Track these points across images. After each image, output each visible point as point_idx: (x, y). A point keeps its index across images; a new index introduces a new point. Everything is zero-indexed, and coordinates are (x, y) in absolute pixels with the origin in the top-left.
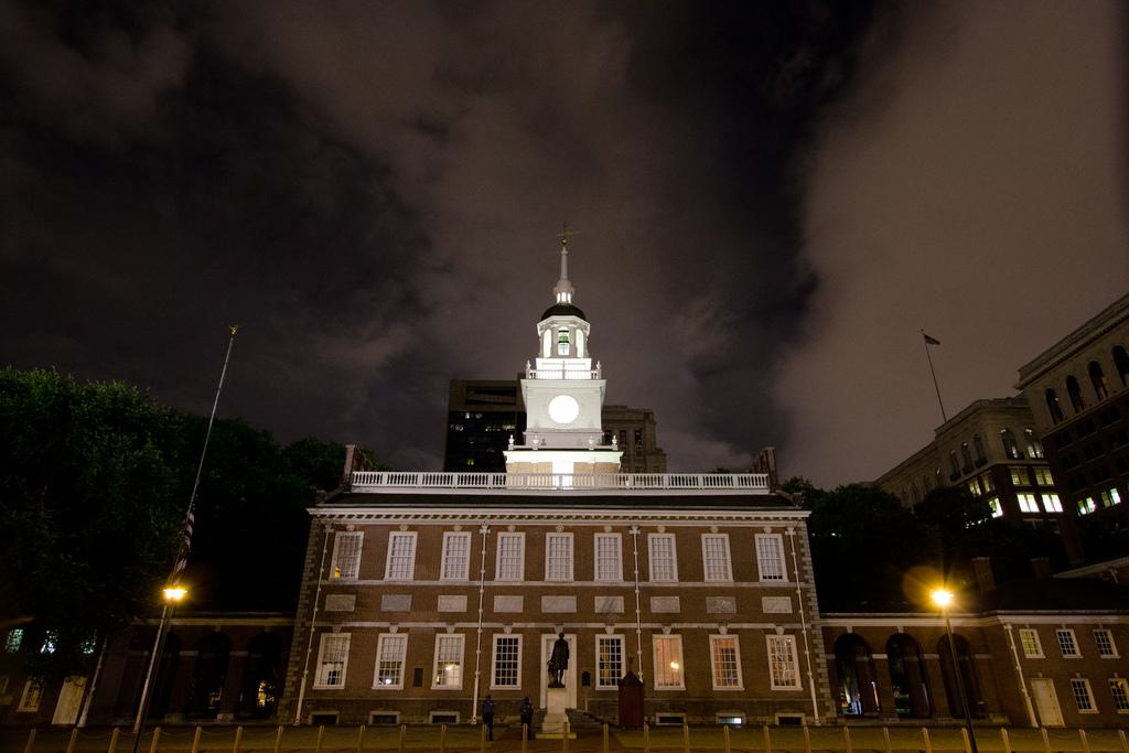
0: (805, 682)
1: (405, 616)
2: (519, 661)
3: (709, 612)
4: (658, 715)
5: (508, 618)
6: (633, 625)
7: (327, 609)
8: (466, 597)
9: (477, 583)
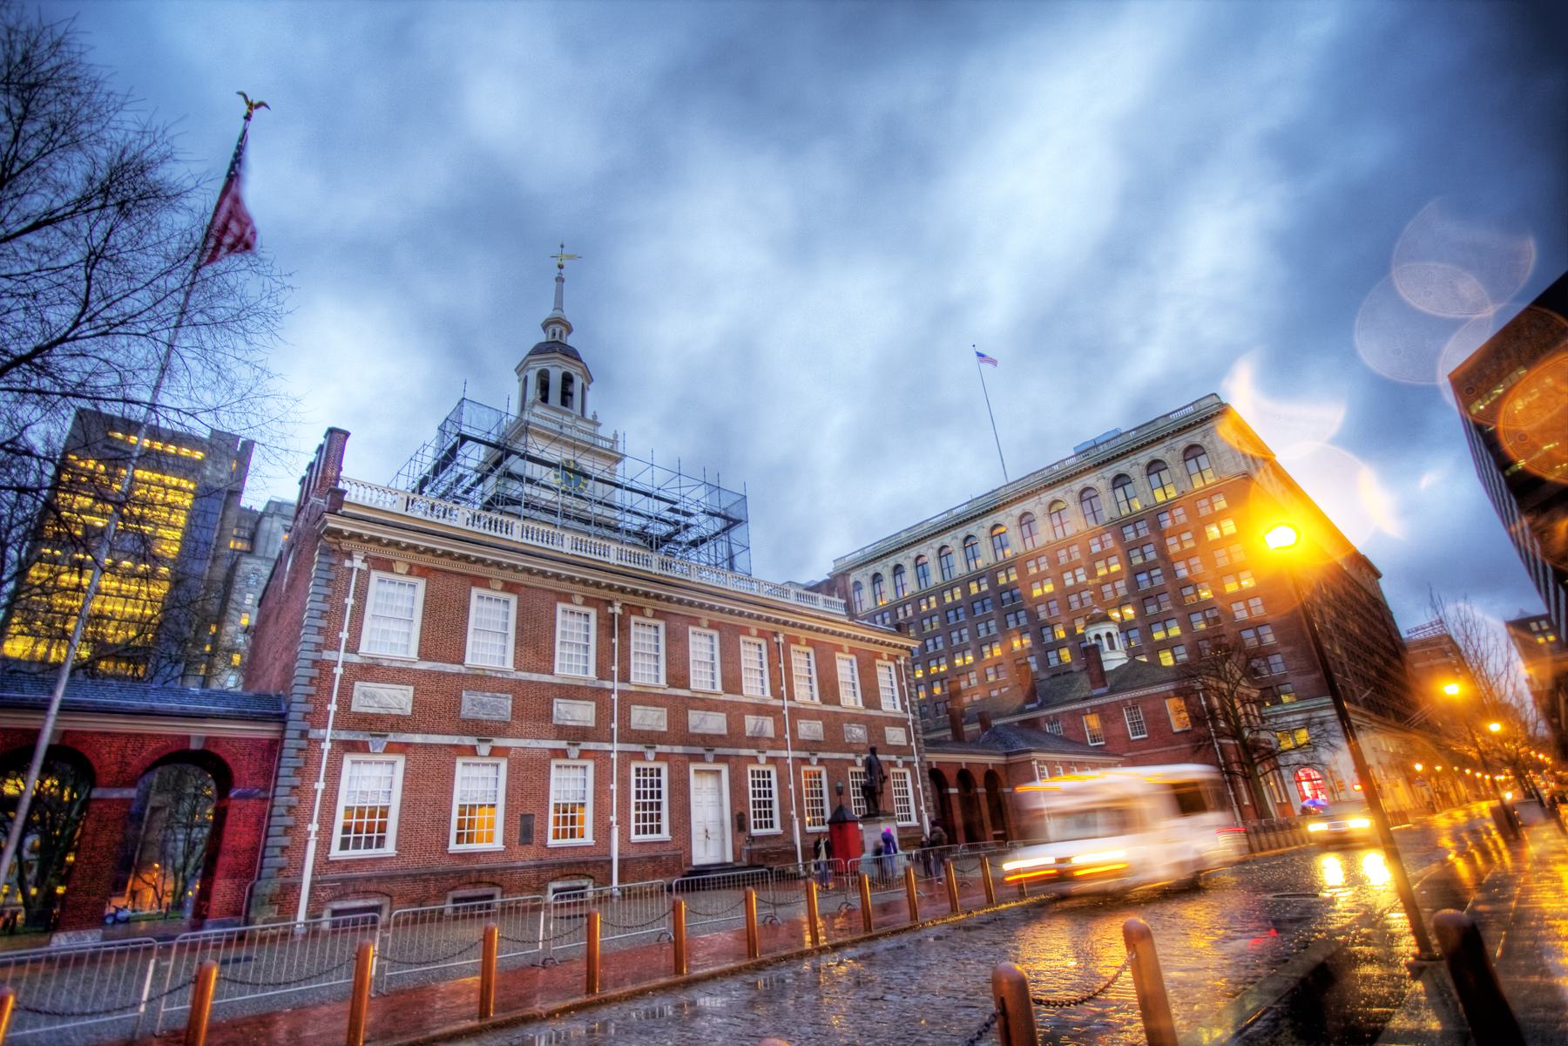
0: (920, 818)
1: (501, 729)
5: (650, 738)
6: (784, 753)
7: (354, 708)
8: (594, 704)
9: (608, 685)
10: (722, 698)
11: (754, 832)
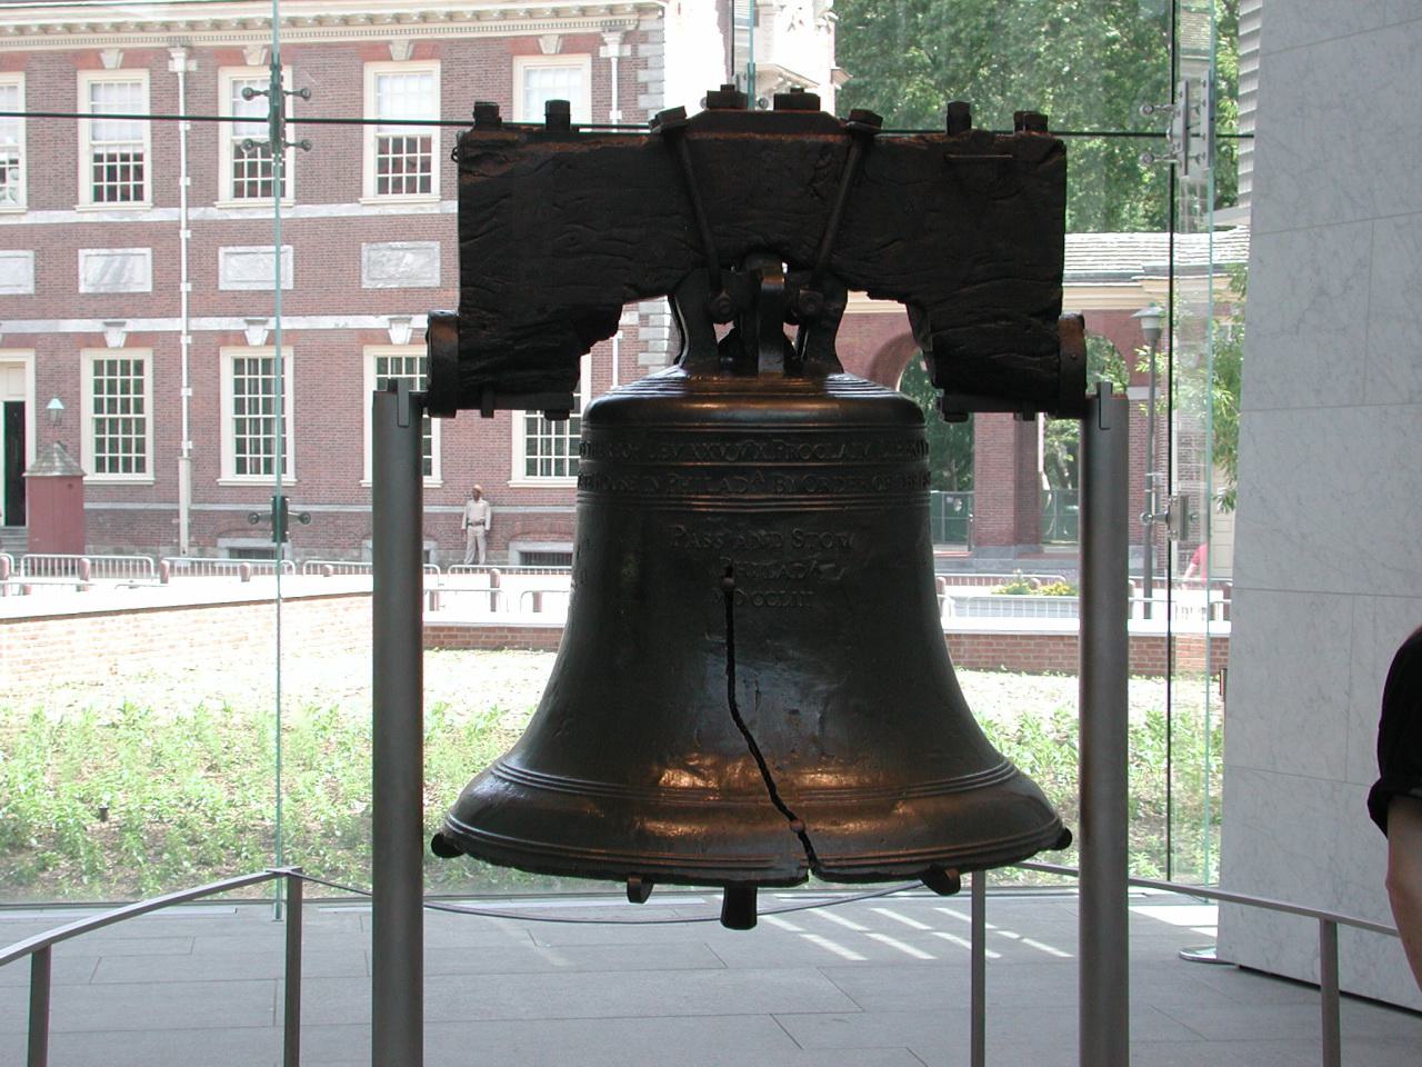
10: (25, 220)
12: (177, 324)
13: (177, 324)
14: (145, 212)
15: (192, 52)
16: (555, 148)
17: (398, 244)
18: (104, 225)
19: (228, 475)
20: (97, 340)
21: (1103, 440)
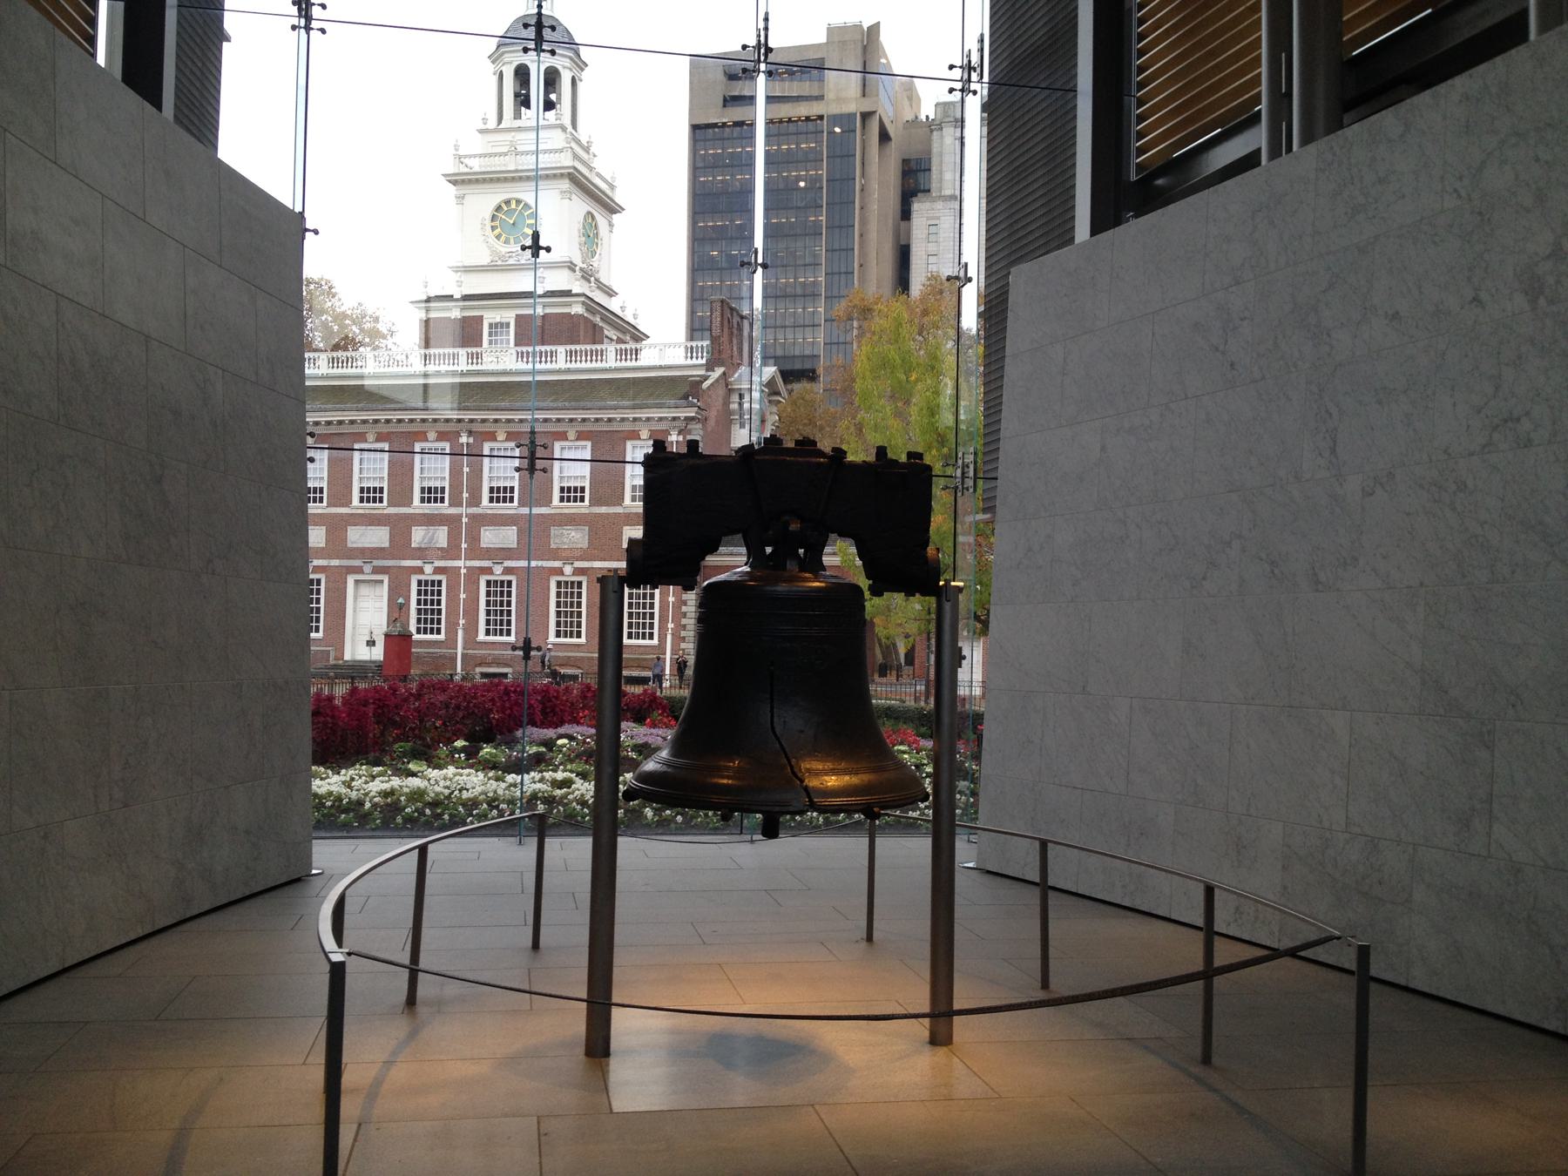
2: (322, 605)
3: (553, 546)
4: (478, 670)
10: (385, 512)
11: (416, 637)
12: (460, 563)
13: (460, 563)
14: (444, 508)
15: (470, 433)
16: (692, 461)
17: (569, 527)
18: (424, 515)
19: (482, 637)
20: (420, 570)
21: (947, 606)
